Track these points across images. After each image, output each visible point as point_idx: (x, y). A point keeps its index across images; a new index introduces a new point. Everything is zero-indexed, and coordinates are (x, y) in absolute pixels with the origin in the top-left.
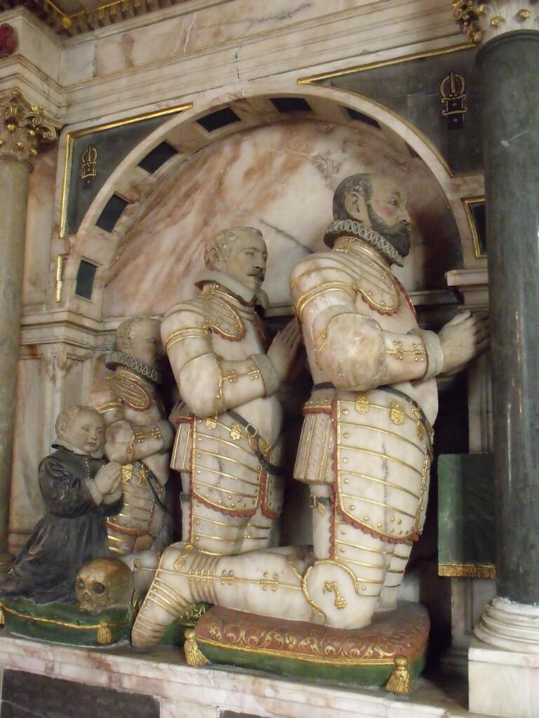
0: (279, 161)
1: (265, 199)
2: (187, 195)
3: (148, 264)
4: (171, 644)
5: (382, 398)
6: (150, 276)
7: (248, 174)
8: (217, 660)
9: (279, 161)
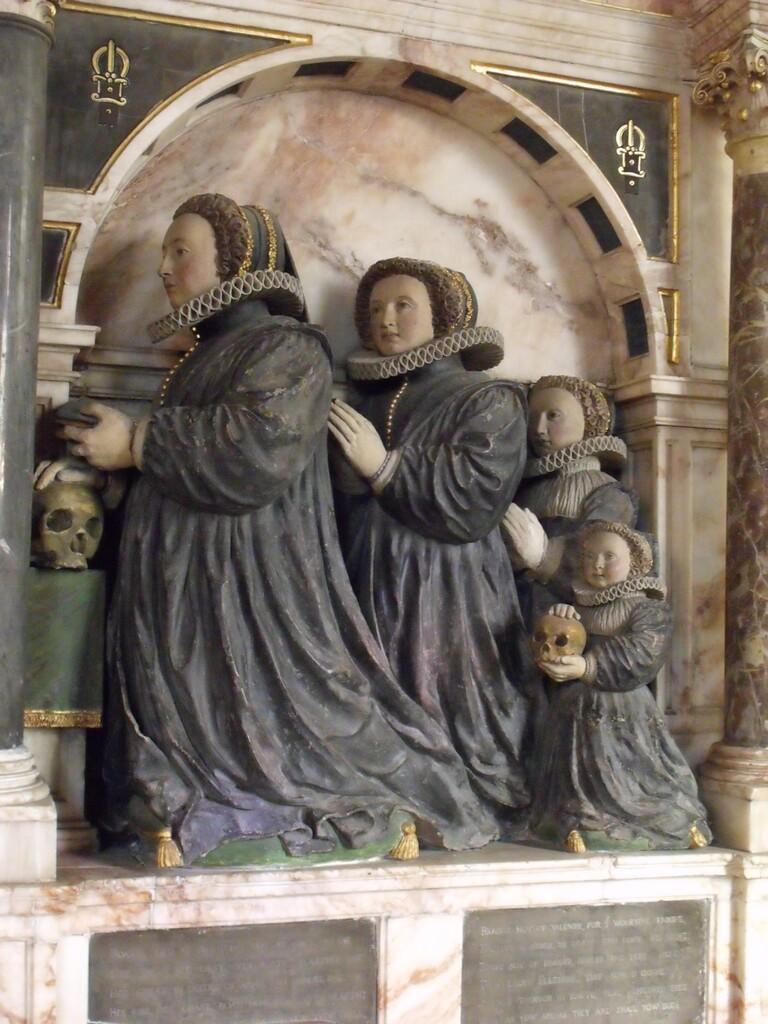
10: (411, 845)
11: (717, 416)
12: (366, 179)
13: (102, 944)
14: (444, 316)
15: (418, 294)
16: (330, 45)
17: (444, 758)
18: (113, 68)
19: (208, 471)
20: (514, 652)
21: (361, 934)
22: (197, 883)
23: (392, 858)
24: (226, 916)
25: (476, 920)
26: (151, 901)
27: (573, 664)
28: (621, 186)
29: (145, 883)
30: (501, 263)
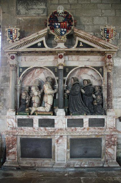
0: (40, 72)
1: (38, 76)
2: (30, 74)
3: (26, 81)
4: (34, 114)
5: (50, 95)
6: (26, 82)
7: (37, 73)
8: (38, 115)
9: (40, 72)
10: (85, 114)
11: (106, 87)
12: (84, 74)
13: (68, 119)
14: (88, 83)
15: (86, 81)
16: (80, 66)
17: (88, 109)
18: (67, 69)
19: (73, 93)
20: (92, 103)
21: (82, 119)
22: (73, 116)
23: (84, 115)
24: (75, 118)
25: (89, 119)
26: (70, 117)
27: (96, 104)
28: (100, 73)
29: (70, 116)
30: (93, 78)
